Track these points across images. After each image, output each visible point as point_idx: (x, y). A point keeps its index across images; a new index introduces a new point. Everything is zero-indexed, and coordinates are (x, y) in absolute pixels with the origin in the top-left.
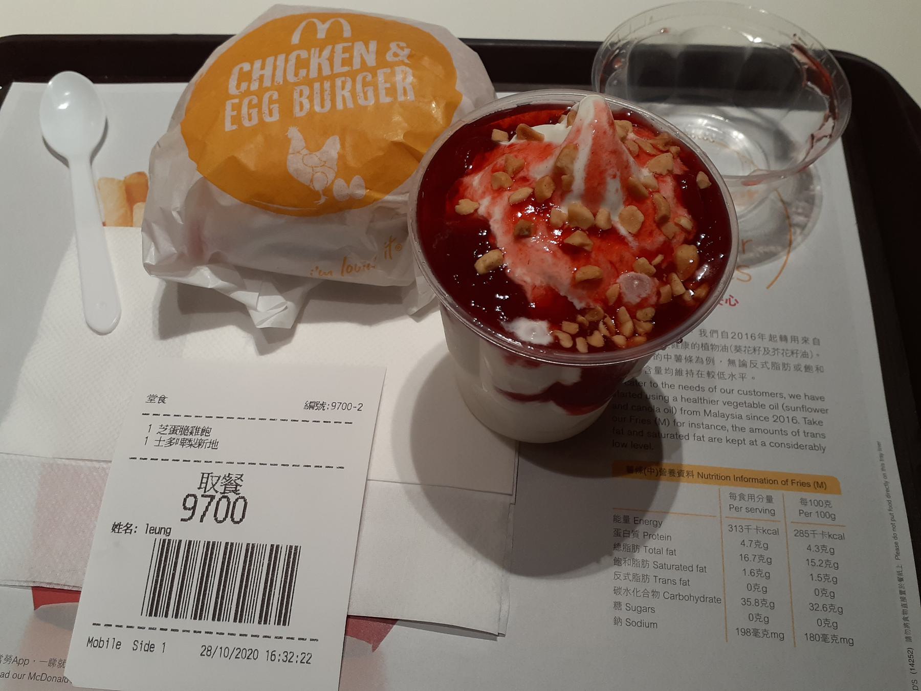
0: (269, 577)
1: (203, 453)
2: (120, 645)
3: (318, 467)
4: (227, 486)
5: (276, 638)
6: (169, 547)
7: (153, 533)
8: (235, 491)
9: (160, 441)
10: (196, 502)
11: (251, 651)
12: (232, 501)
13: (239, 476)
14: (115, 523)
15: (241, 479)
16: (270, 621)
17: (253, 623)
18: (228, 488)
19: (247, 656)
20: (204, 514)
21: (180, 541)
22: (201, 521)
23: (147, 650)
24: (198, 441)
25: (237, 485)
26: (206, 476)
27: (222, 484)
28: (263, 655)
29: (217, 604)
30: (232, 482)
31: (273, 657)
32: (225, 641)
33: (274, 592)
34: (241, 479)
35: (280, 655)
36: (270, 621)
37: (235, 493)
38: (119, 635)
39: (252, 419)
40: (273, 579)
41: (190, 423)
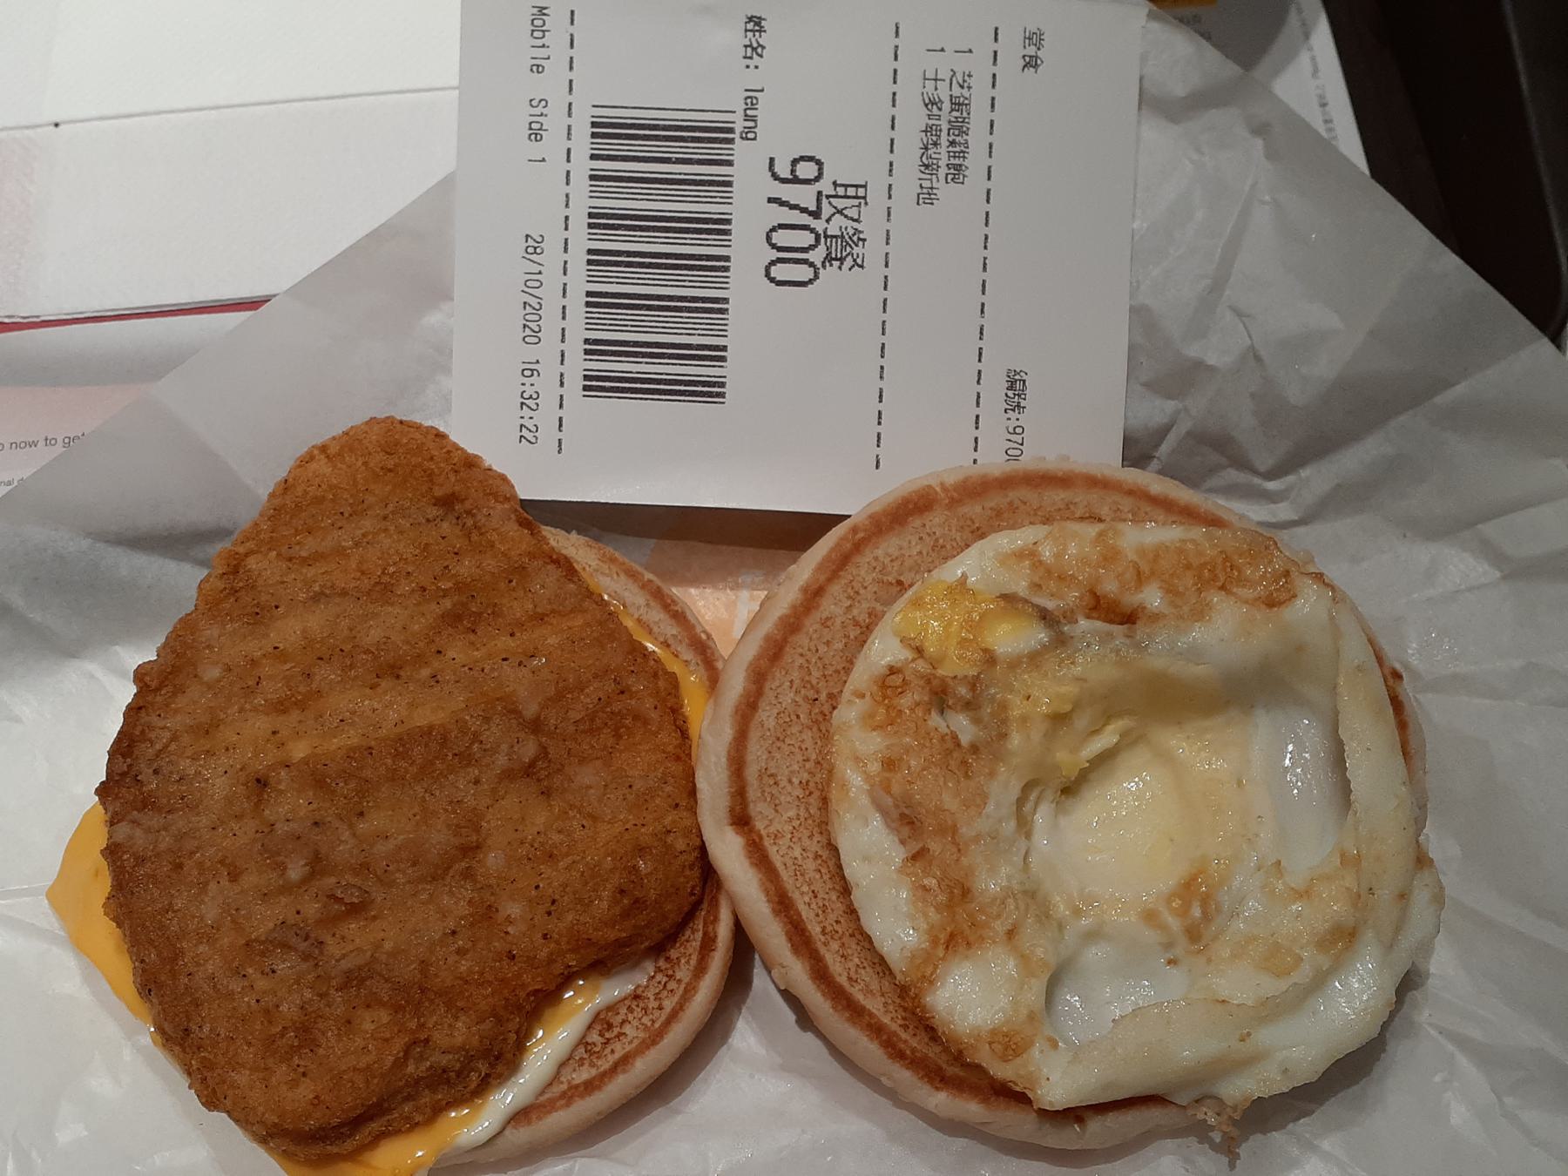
0: (668, 348)
1: (908, 177)
2: (538, 72)
3: (880, 417)
4: (839, 240)
5: (562, 375)
6: (720, 143)
7: (747, 104)
8: (829, 259)
9: (936, 80)
10: (807, 182)
11: (537, 330)
12: (811, 256)
13: (859, 261)
14: (764, 19)
15: (853, 266)
16: (591, 360)
17: (587, 329)
18: (836, 243)
19: (528, 323)
20: (782, 203)
21: (730, 163)
22: (770, 200)
23: (531, 129)
24: (935, 161)
25: (842, 260)
26: (861, 192)
27: (843, 230)
28: (531, 353)
29: (618, 256)
30: (848, 249)
31: (529, 373)
32: (552, 278)
33: (641, 363)
34: (853, 266)
35: (532, 385)
36: (591, 360)
37: (825, 259)
38: (556, 69)
39: (985, 264)
40: (664, 358)
41: (977, 137)
